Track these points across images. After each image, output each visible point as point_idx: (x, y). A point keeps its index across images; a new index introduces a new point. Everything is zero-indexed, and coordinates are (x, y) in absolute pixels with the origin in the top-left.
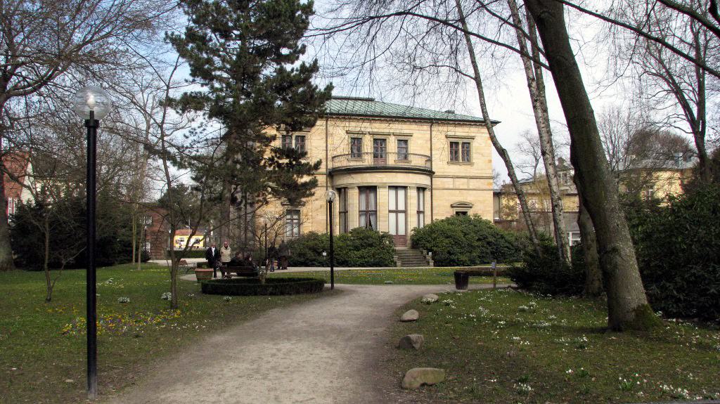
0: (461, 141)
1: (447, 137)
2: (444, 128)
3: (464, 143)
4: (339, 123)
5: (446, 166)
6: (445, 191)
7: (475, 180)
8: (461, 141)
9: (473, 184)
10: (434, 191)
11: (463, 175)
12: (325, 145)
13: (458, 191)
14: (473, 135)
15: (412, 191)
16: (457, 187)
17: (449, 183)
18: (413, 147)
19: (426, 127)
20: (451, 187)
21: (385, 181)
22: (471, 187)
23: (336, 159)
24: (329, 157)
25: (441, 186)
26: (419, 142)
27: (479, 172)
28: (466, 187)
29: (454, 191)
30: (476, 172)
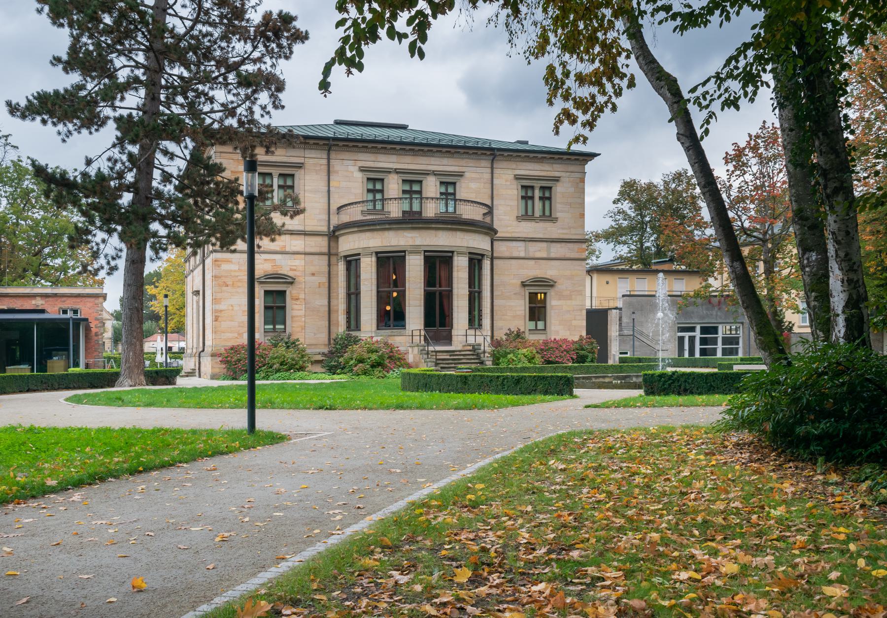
0: (537, 184)
1: (517, 178)
2: (513, 165)
3: (543, 188)
4: (346, 155)
5: (515, 223)
6: (513, 261)
7: (558, 245)
8: (537, 184)
9: (557, 250)
10: (496, 262)
11: (541, 236)
12: (327, 188)
13: (532, 262)
14: (557, 174)
15: (460, 258)
16: (531, 255)
17: (519, 249)
18: (464, 190)
19: (486, 163)
20: (522, 254)
21: (418, 243)
22: (553, 255)
23: (344, 211)
24: (334, 207)
25: (507, 254)
26: (473, 185)
27: (565, 231)
28: (544, 255)
29: (526, 261)
30: (560, 231)
